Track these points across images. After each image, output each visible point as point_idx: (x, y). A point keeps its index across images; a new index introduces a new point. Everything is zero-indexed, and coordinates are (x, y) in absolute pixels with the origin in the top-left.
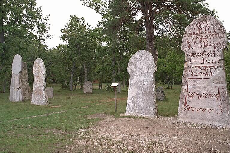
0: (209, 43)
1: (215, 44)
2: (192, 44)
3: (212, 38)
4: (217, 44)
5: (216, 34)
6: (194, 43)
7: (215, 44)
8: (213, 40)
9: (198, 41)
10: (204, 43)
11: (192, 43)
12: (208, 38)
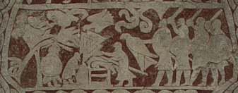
0: (164, 65)
1: (205, 74)
2: (49, 67)
3: (182, 32)
5: (208, 14)
6: (65, 56)
7: (205, 74)
8: (187, 48)
9: (91, 41)
10: (133, 62)
11: (44, 52)
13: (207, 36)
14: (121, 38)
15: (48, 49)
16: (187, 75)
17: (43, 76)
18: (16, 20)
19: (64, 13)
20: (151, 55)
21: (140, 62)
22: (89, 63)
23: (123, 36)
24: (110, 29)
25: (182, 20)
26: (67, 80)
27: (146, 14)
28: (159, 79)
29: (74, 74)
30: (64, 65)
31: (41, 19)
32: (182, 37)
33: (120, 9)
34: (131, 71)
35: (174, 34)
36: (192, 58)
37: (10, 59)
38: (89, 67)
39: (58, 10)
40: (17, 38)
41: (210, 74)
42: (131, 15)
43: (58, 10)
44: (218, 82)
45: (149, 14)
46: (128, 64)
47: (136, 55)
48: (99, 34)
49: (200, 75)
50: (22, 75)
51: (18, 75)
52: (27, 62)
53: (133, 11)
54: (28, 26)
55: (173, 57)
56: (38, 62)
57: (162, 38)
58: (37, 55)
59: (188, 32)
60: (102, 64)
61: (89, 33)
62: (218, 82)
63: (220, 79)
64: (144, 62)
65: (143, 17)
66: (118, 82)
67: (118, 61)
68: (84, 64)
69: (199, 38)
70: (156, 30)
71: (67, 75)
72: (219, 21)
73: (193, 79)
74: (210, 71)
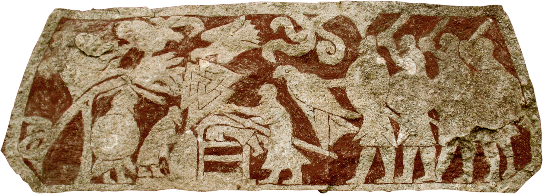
0: (375, 132)
1: (467, 154)
3: (412, 63)
4: (493, 163)
6: (147, 114)
8: (425, 98)
11: (102, 106)
12: (351, 57)
13: (464, 70)
14: (275, 76)
15: (111, 98)
16: (428, 156)
17: (94, 157)
18: (52, 40)
19: (154, 24)
20: (344, 112)
21: (320, 128)
22: (200, 129)
23: (280, 72)
24: (253, 55)
25: (408, 39)
26: (149, 168)
27: (331, 26)
28: (362, 170)
29: (164, 153)
30: (144, 135)
31: (103, 38)
32: (412, 72)
33: (274, 16)
34: (299, 149)
35: (393, 68)
36: (437, 119)
37: (29, 119)
38: (200, 139)
39: (141, 18)
40: (48, 75)
41: (480, 154)
42: (298, 28)
43: (141, 18)
44: (501, 173)
45: (336, 26)
46: (290, 130)
47: (306, 110)
48: (225, 66)
49: (457, 157)
50: (48, 155)
51: (38, 155)
52: (62, 127)
53: (301, 20)
54: (74, 52)
55: (394, 116)
56: (87, 128)
57: (367, 77)
58: (87, 114)
59: (423, 65)
60: (230, 132)
61: (204, 65)
62: (501, 173)
63: (503, 165)
64: (329, 130)
65: (324, 33)
66: (268, 173)
67: (267, 126)
68: (188, 132)
69: (449, 76)
70: (355, 57)
71: (149, 157)
72: (488, 43)
73: (442, 167)
74: (479, 147)
